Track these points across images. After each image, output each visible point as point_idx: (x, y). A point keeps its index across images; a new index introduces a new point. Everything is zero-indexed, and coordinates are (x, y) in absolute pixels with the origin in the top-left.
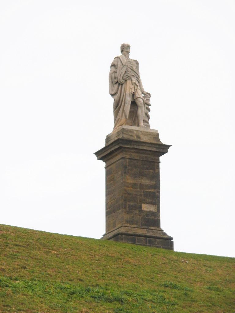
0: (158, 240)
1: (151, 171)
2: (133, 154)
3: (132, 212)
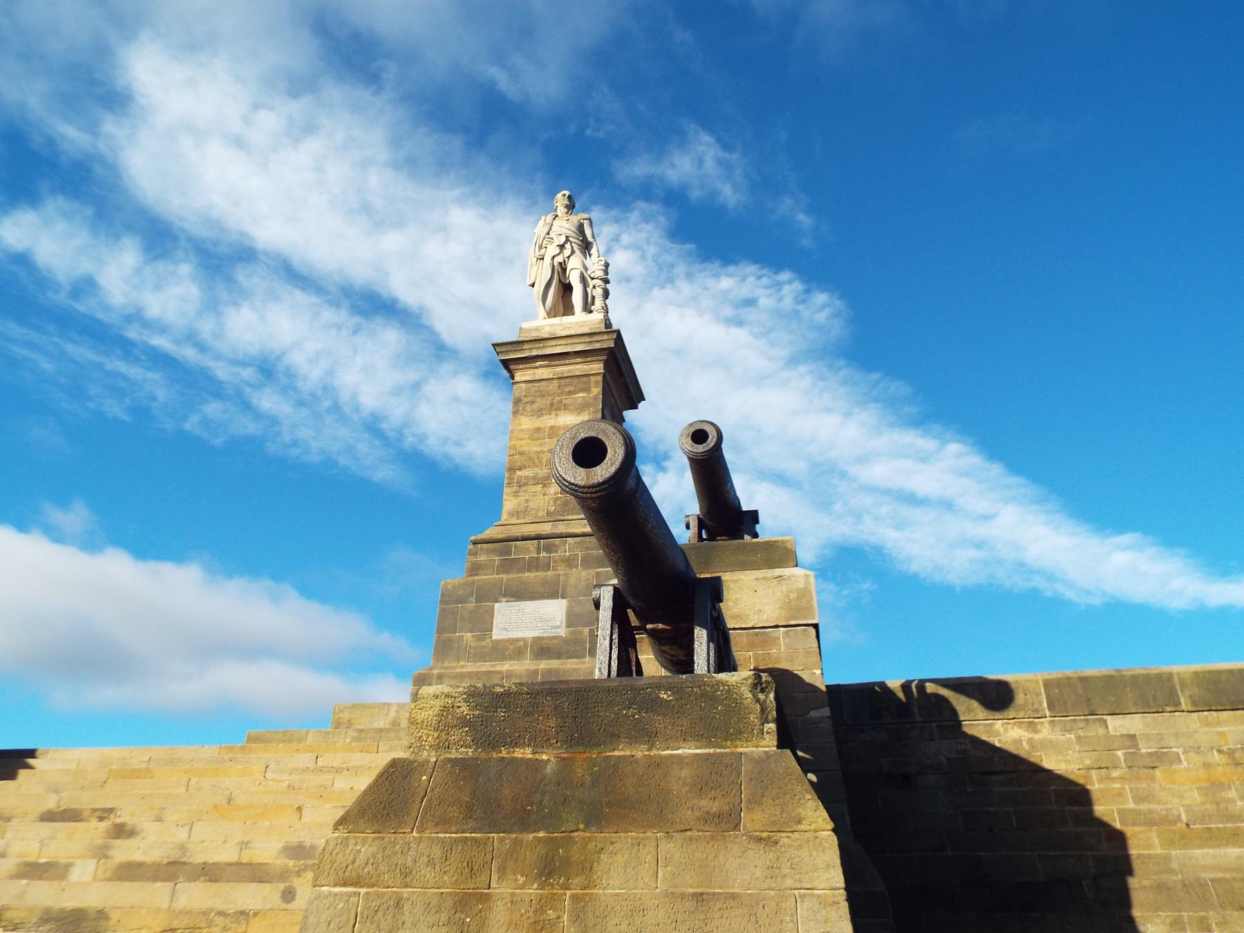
0: (569, 540)
3: (526, 491)
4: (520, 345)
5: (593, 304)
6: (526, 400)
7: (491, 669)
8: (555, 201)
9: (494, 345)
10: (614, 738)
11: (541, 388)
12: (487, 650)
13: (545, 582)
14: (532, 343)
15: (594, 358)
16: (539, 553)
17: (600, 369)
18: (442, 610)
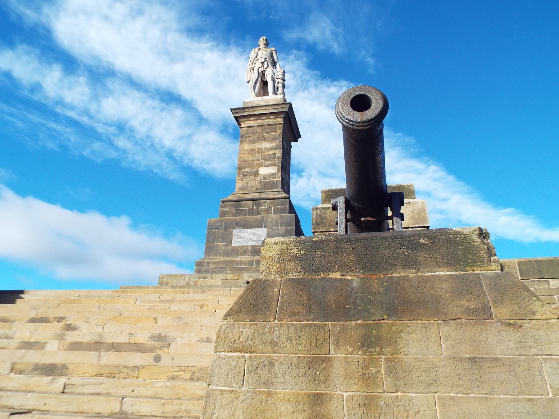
1: (272, 133)
2: (253, 122)
3: (246, 178)
4: (243, 110)
5: (278, 91)
6: (246, 136)
7: (232, 260)
8: (259, 42)
9: (231, 110)
10: (393, 266)
11: (253, 130)
12: (230, 251)
13: (257, 220)
14: (249, 108)
15: (278, 116)
16: (253, 207)
17: (281, 121)
18: (208, 232)
